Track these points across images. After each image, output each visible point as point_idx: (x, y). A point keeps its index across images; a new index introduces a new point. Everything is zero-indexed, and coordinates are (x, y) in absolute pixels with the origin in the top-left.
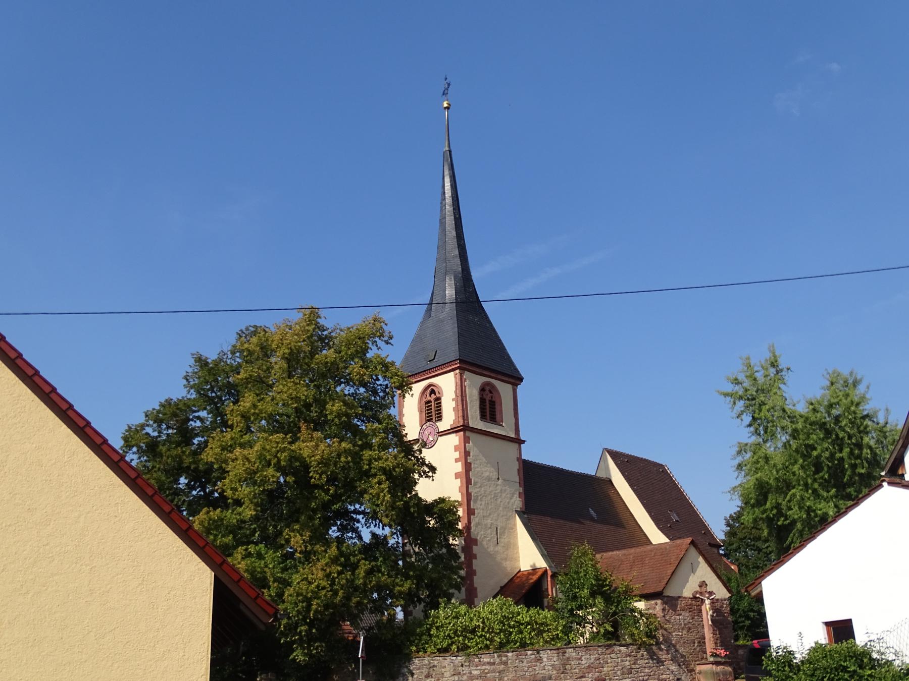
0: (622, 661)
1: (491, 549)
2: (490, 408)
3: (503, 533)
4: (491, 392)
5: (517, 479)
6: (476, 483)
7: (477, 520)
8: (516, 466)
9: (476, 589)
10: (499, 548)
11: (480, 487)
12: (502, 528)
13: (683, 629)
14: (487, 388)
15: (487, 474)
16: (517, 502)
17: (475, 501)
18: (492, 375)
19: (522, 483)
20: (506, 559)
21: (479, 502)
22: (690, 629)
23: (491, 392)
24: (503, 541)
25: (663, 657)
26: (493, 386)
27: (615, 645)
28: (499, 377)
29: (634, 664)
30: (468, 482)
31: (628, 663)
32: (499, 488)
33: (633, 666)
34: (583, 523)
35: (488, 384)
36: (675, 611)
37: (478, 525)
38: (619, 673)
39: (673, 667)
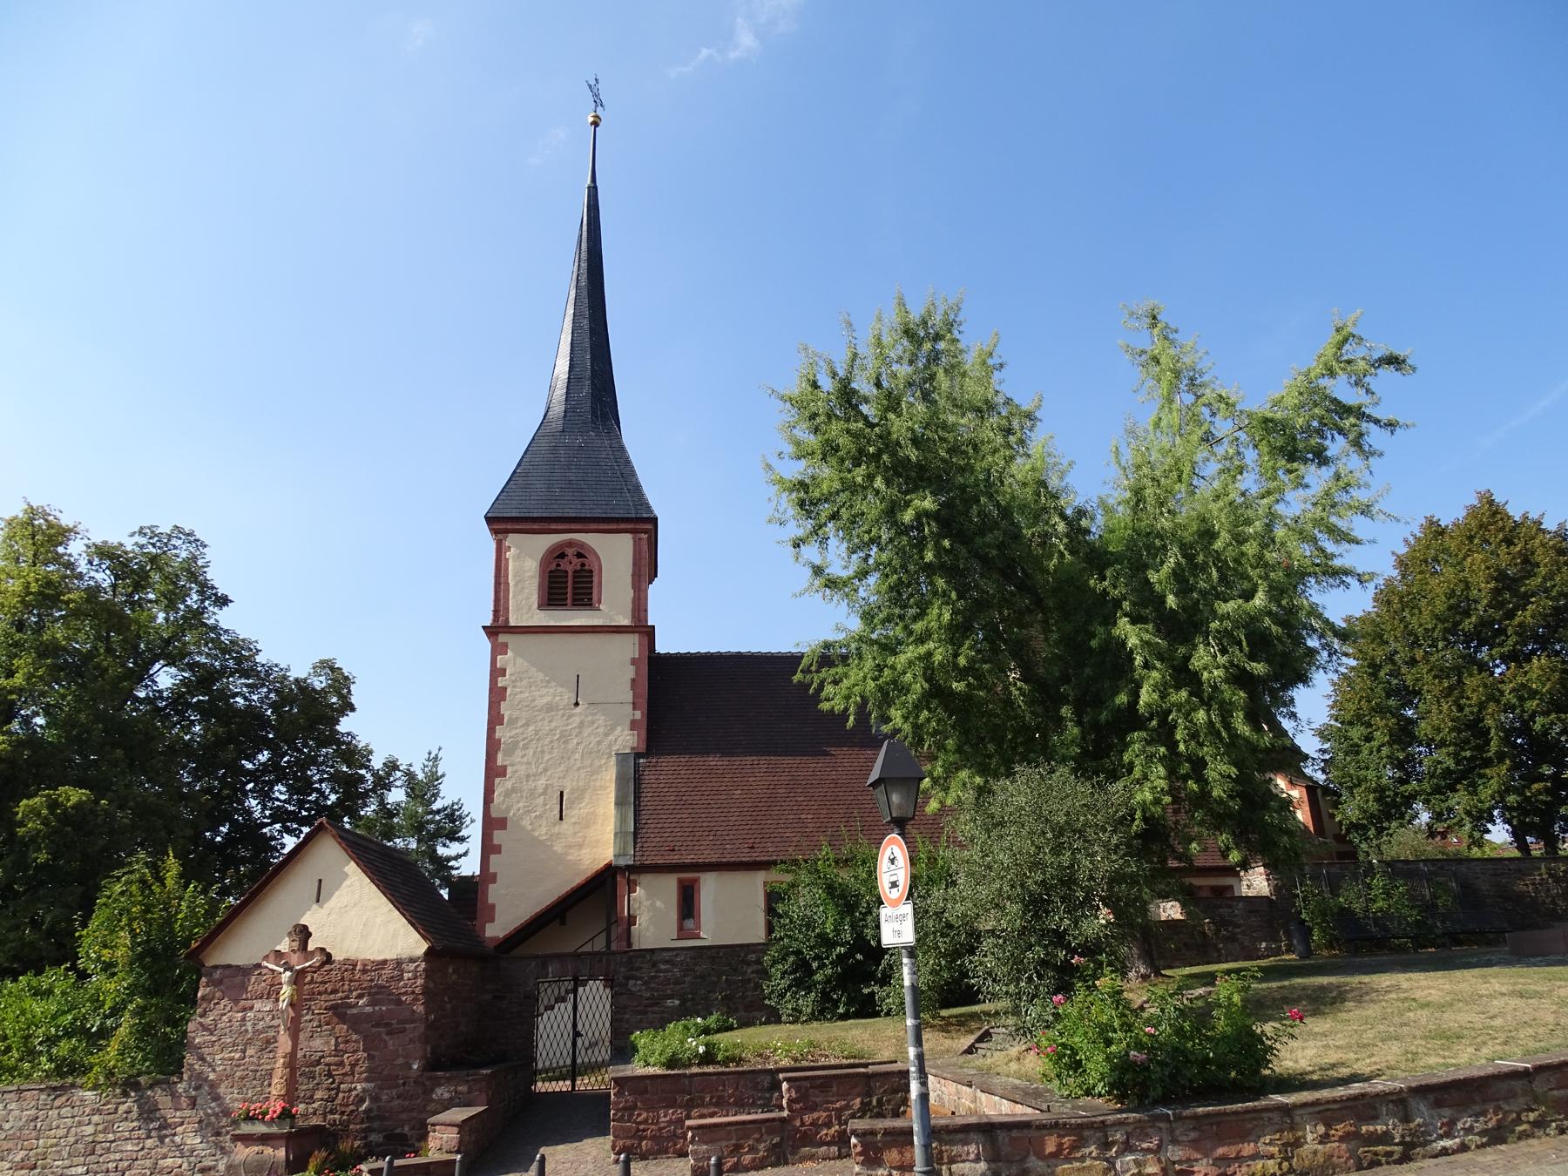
0: (80, 1124)
1: (542, 832)
2: (568, 583)
3: (572, 802)
4: (579, 555)
5: (629, 696)
6: (513, 721)
7: (509, 785)
8: (630, 672)
9: (493, 906)
10: (565, 826)
11: (527, 725)
12: (573, 791)
13: (249, 1042)
14: (570, 552)
15: (547, 699)
16: (626, 739)
17: (510, 753)
18: (573, 526)
19: (644, 702)
20: (580, 846)
21: (519, 753)
22: (268, 1042)
23: (579, 555)
24: (571, 814)
25: (173, 1116)
26: (582, 545)
27: (73, 1086)
28: (594, 526)
29: (104, 1131)
30: (495, 719)
31: (90, 1129)
32: (577, 720)
33: (100, 1137)
34: (827, 754)
35: (570, 544)
36: (236, 1001)
37: (507, 794)
38: (65, 1154)
39: (194, 1140)
